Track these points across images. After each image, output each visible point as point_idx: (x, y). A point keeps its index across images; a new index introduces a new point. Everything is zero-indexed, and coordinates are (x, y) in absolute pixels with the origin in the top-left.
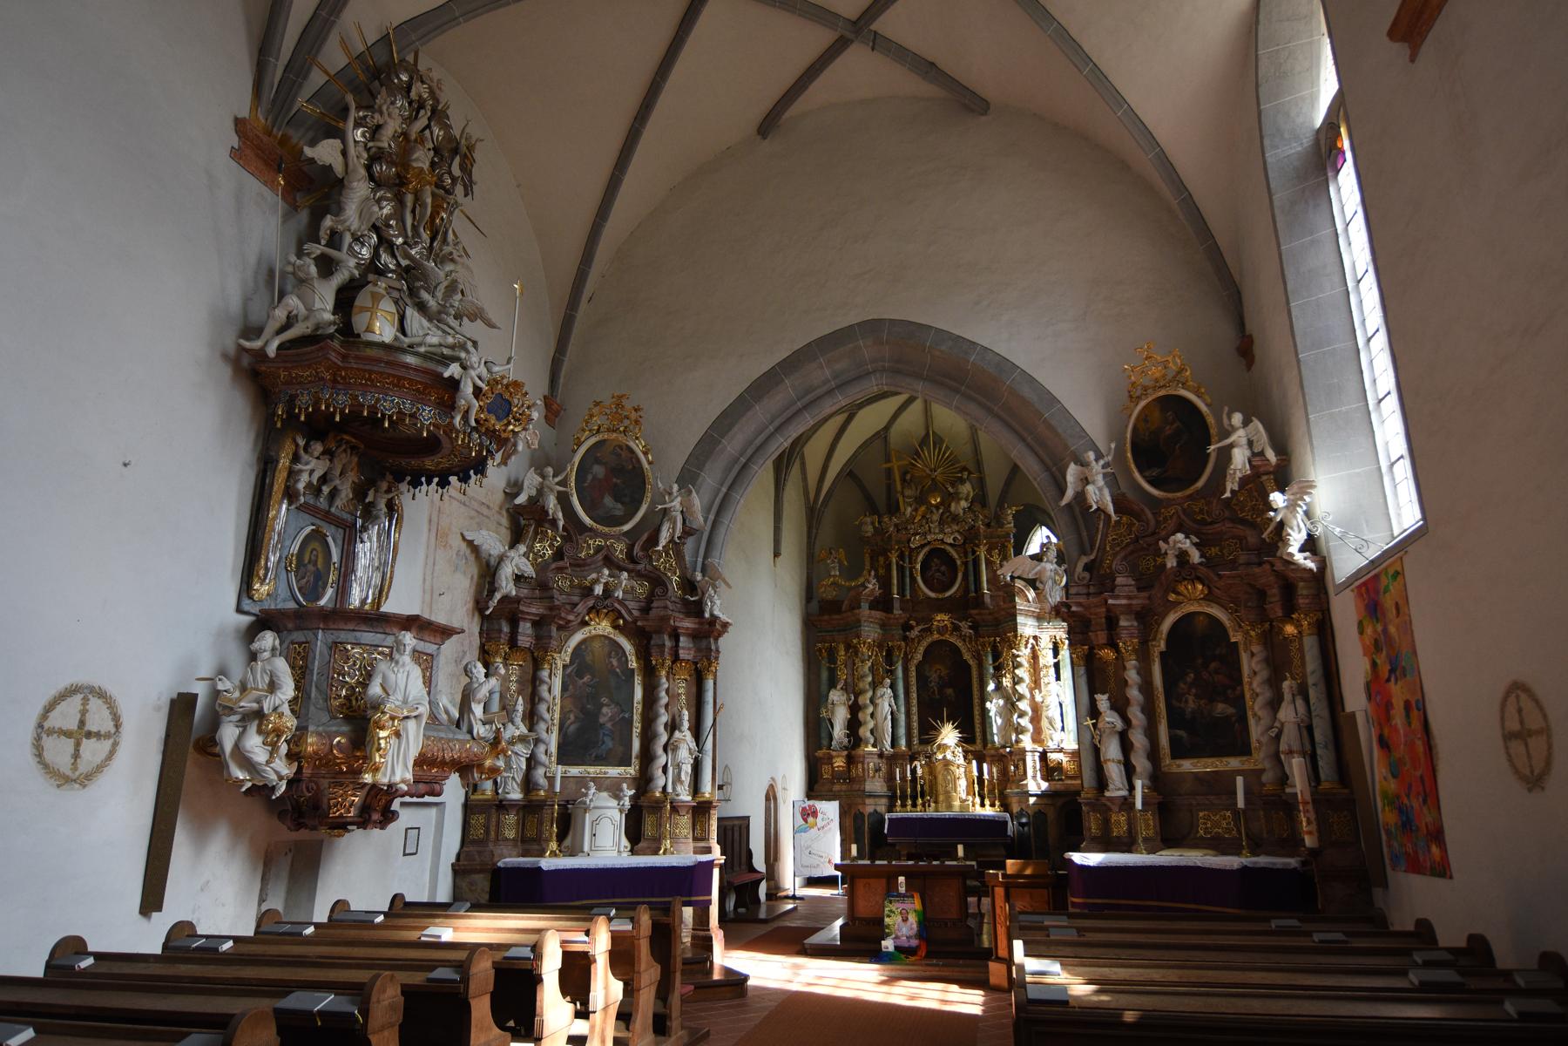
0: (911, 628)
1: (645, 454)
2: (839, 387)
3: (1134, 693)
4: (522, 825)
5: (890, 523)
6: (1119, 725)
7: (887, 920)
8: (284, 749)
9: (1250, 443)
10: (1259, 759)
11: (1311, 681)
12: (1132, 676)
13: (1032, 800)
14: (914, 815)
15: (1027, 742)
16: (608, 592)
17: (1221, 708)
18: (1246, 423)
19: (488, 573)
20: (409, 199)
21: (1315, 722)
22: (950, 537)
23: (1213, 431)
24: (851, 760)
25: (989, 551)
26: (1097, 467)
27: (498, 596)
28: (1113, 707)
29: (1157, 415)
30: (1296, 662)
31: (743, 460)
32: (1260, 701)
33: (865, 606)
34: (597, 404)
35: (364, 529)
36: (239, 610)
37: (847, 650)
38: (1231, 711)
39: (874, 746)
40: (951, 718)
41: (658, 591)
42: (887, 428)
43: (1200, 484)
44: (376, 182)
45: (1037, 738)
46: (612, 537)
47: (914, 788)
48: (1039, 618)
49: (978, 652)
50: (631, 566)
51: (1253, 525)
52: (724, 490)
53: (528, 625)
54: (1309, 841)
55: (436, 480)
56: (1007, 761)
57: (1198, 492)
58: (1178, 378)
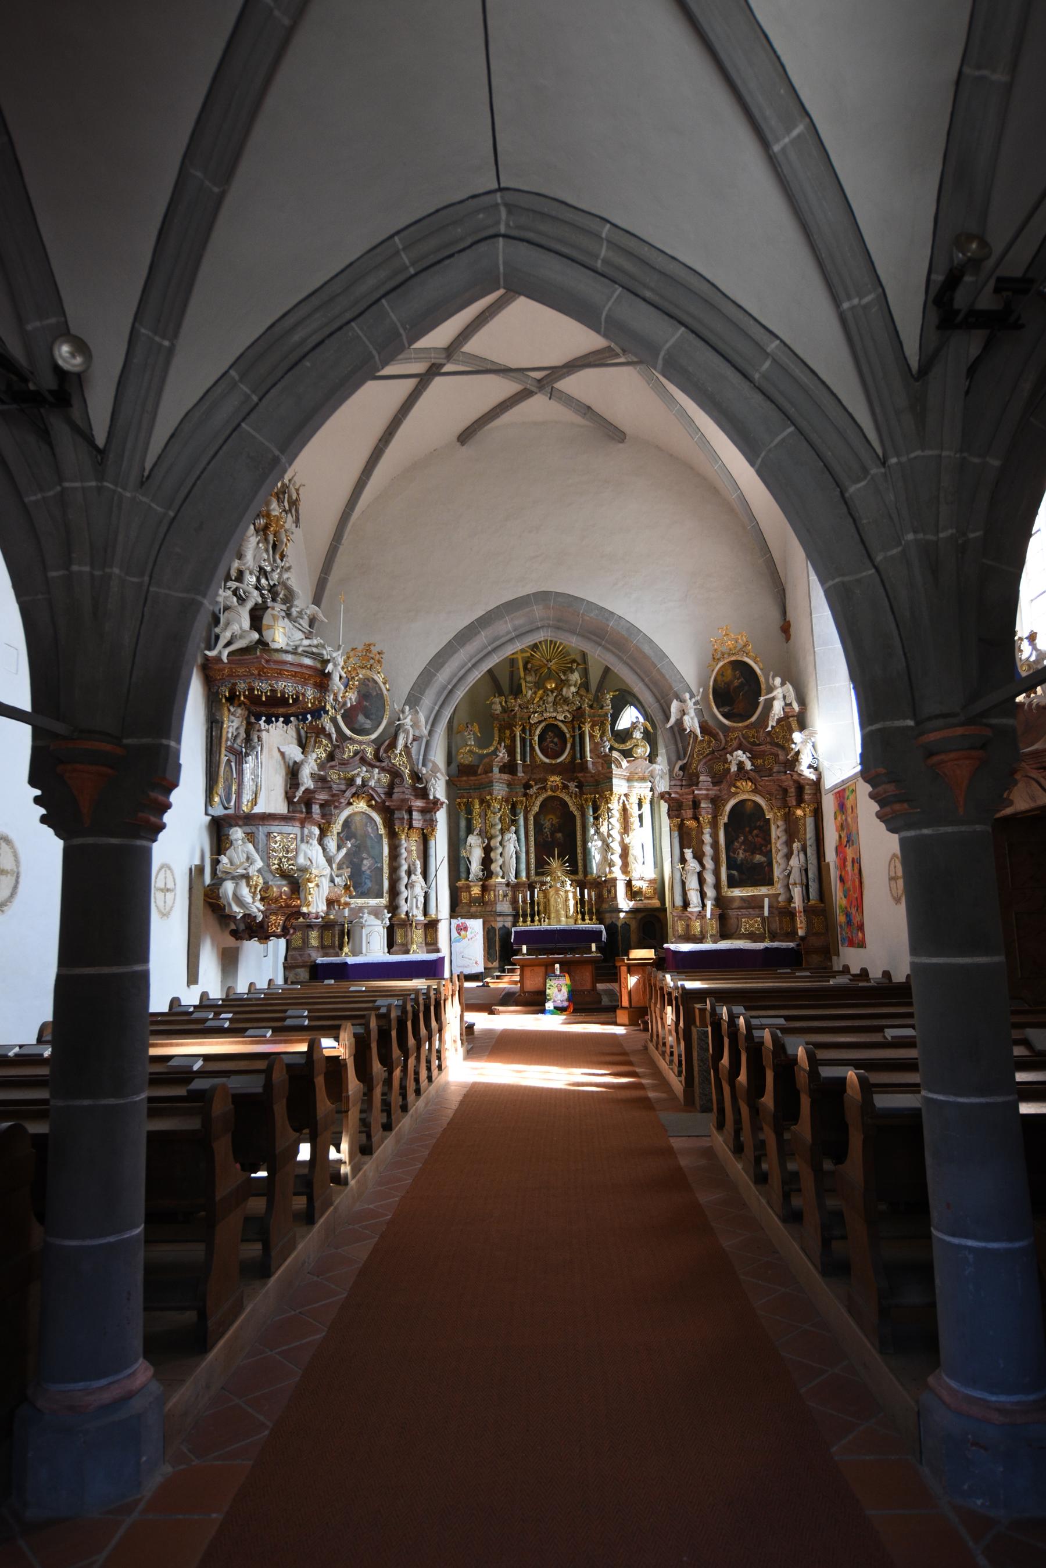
0: (531, 787)
1: (385, 683)
2: (517, 636)
3: (708, 850)
4: (321, 938)
5: (515, 704)
6: (698, 869)
7: (548, 991)
8: (259, 897)
9: (784, 697)
10: (778, 888)
11: (808, 843)
12: (707, 838)
13: (622, 915)
14: (533, 928)
15: (617, 872)
16: (364, 784)
17: (758, 858)
18: (783, 684)
19: (293, 773)
20: (271, 538)
21: (809, 866)
23: (763, 686)
24: (485, 889)
25: (592, 727)
26: (690, 703)
27: (302, 789)
28: (695, 857)
29: (729, 672)
30: (802, 831)
31: (450, 687)
32: (780, 854)
33: (496, 770)
34: (353, 649)
35: (247, 755)
36: (207, 814)
37: (481, 804)
38: (763, 859)
39: (503, 877)
41: (397, 780)
43: (753, 719)
44: (257, 531)
45: (625, 868)
46: (364, 743)
47: (532, 908)
48: (629, 780)
49: (582, 806)
50: (378, 764)
51: (783, 748)
52: (437, 708)
53: (317, 807)
54: (801, 932)
55: (281, 719)
56: (604, 887)
57: (752, 724)
58: (743, 650)
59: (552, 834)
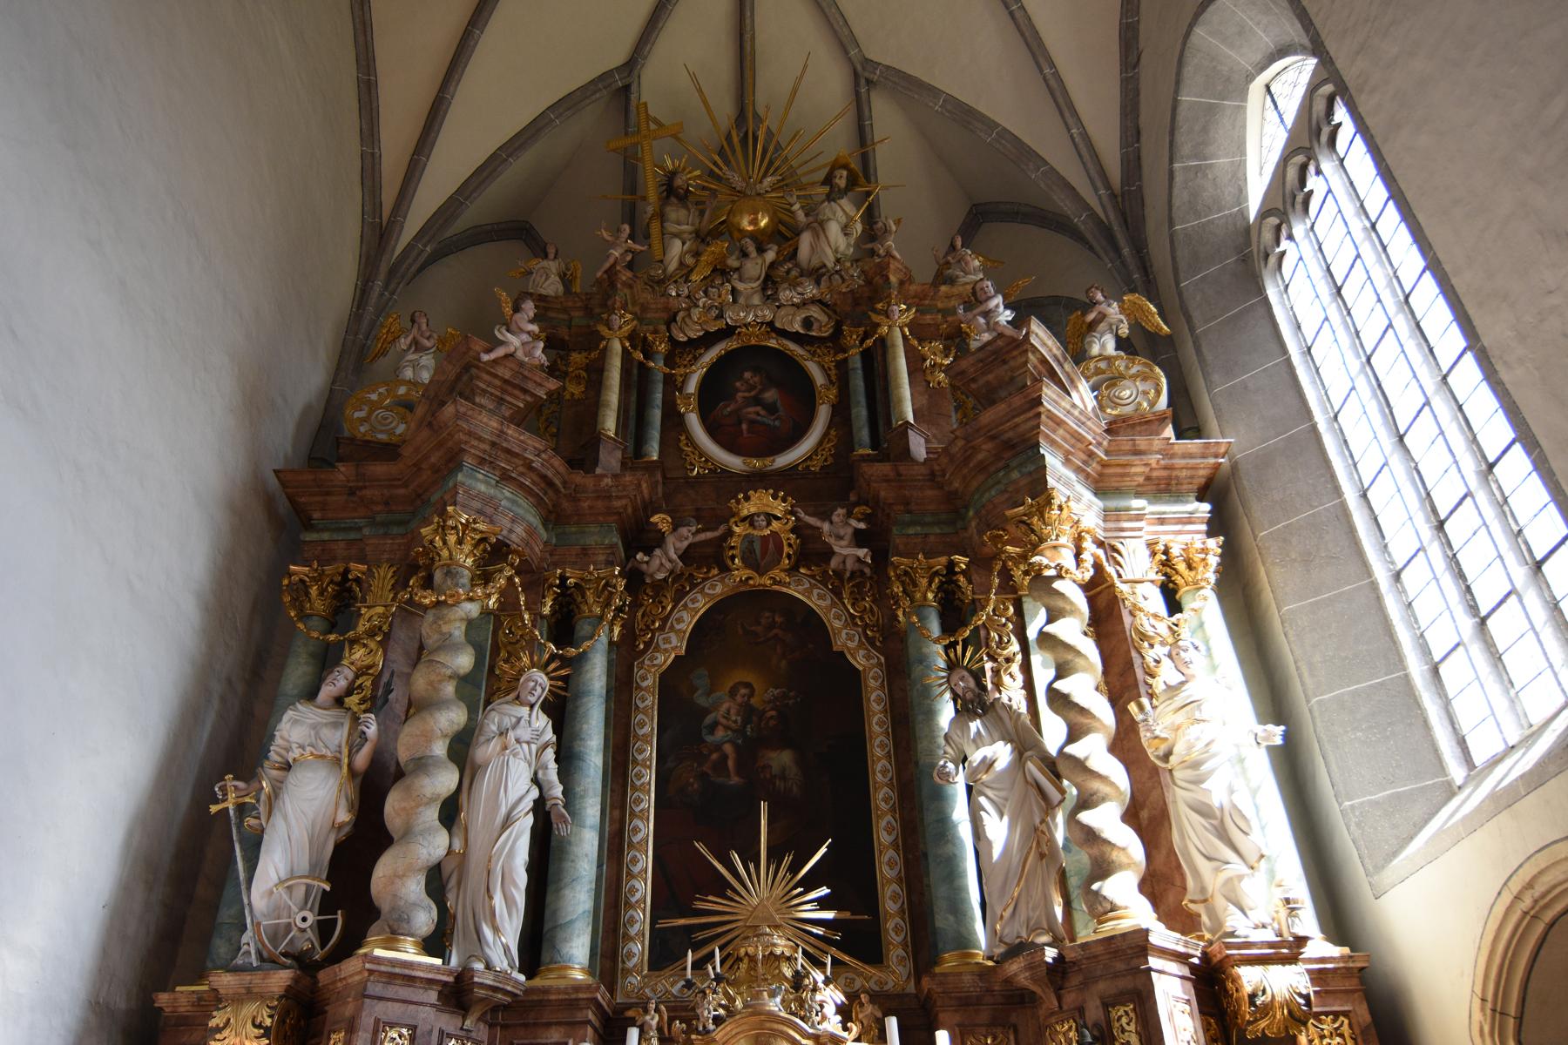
22: (796, 308)
39: (435, 944)
40: (789, 847)
42: (631, 65)
59: (749, 751)
